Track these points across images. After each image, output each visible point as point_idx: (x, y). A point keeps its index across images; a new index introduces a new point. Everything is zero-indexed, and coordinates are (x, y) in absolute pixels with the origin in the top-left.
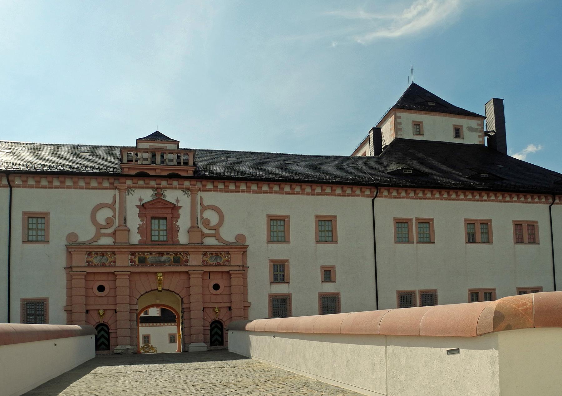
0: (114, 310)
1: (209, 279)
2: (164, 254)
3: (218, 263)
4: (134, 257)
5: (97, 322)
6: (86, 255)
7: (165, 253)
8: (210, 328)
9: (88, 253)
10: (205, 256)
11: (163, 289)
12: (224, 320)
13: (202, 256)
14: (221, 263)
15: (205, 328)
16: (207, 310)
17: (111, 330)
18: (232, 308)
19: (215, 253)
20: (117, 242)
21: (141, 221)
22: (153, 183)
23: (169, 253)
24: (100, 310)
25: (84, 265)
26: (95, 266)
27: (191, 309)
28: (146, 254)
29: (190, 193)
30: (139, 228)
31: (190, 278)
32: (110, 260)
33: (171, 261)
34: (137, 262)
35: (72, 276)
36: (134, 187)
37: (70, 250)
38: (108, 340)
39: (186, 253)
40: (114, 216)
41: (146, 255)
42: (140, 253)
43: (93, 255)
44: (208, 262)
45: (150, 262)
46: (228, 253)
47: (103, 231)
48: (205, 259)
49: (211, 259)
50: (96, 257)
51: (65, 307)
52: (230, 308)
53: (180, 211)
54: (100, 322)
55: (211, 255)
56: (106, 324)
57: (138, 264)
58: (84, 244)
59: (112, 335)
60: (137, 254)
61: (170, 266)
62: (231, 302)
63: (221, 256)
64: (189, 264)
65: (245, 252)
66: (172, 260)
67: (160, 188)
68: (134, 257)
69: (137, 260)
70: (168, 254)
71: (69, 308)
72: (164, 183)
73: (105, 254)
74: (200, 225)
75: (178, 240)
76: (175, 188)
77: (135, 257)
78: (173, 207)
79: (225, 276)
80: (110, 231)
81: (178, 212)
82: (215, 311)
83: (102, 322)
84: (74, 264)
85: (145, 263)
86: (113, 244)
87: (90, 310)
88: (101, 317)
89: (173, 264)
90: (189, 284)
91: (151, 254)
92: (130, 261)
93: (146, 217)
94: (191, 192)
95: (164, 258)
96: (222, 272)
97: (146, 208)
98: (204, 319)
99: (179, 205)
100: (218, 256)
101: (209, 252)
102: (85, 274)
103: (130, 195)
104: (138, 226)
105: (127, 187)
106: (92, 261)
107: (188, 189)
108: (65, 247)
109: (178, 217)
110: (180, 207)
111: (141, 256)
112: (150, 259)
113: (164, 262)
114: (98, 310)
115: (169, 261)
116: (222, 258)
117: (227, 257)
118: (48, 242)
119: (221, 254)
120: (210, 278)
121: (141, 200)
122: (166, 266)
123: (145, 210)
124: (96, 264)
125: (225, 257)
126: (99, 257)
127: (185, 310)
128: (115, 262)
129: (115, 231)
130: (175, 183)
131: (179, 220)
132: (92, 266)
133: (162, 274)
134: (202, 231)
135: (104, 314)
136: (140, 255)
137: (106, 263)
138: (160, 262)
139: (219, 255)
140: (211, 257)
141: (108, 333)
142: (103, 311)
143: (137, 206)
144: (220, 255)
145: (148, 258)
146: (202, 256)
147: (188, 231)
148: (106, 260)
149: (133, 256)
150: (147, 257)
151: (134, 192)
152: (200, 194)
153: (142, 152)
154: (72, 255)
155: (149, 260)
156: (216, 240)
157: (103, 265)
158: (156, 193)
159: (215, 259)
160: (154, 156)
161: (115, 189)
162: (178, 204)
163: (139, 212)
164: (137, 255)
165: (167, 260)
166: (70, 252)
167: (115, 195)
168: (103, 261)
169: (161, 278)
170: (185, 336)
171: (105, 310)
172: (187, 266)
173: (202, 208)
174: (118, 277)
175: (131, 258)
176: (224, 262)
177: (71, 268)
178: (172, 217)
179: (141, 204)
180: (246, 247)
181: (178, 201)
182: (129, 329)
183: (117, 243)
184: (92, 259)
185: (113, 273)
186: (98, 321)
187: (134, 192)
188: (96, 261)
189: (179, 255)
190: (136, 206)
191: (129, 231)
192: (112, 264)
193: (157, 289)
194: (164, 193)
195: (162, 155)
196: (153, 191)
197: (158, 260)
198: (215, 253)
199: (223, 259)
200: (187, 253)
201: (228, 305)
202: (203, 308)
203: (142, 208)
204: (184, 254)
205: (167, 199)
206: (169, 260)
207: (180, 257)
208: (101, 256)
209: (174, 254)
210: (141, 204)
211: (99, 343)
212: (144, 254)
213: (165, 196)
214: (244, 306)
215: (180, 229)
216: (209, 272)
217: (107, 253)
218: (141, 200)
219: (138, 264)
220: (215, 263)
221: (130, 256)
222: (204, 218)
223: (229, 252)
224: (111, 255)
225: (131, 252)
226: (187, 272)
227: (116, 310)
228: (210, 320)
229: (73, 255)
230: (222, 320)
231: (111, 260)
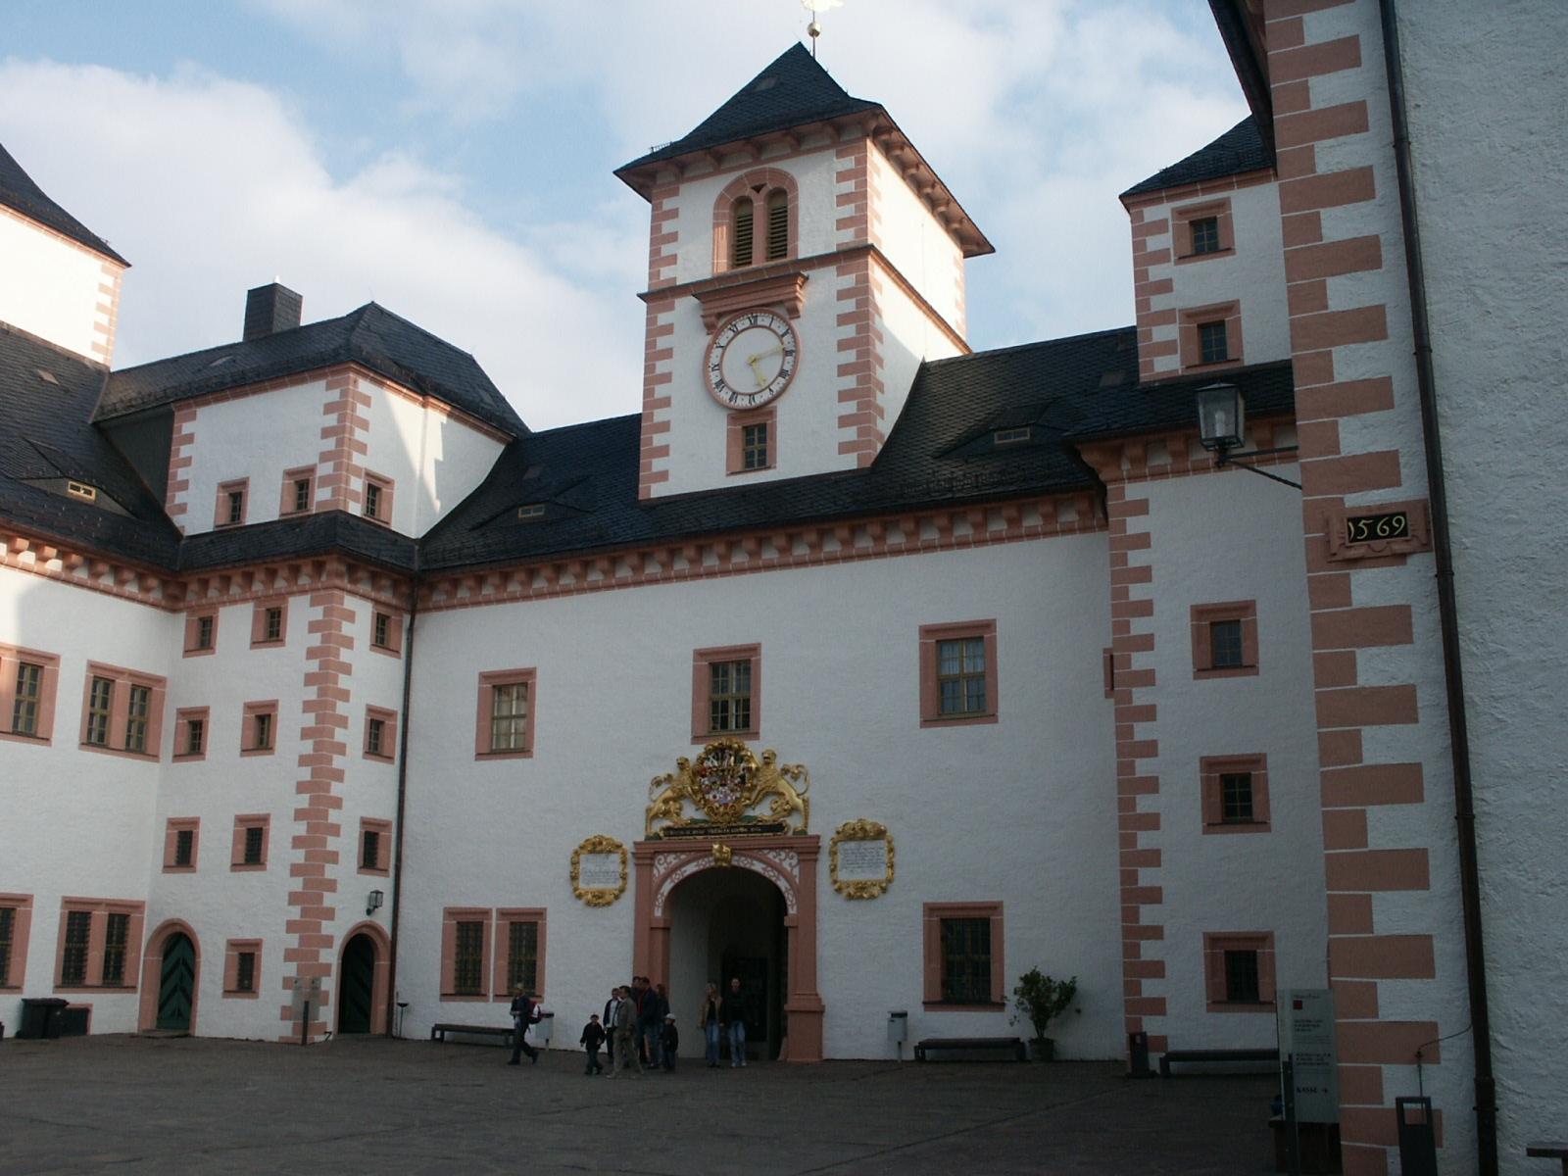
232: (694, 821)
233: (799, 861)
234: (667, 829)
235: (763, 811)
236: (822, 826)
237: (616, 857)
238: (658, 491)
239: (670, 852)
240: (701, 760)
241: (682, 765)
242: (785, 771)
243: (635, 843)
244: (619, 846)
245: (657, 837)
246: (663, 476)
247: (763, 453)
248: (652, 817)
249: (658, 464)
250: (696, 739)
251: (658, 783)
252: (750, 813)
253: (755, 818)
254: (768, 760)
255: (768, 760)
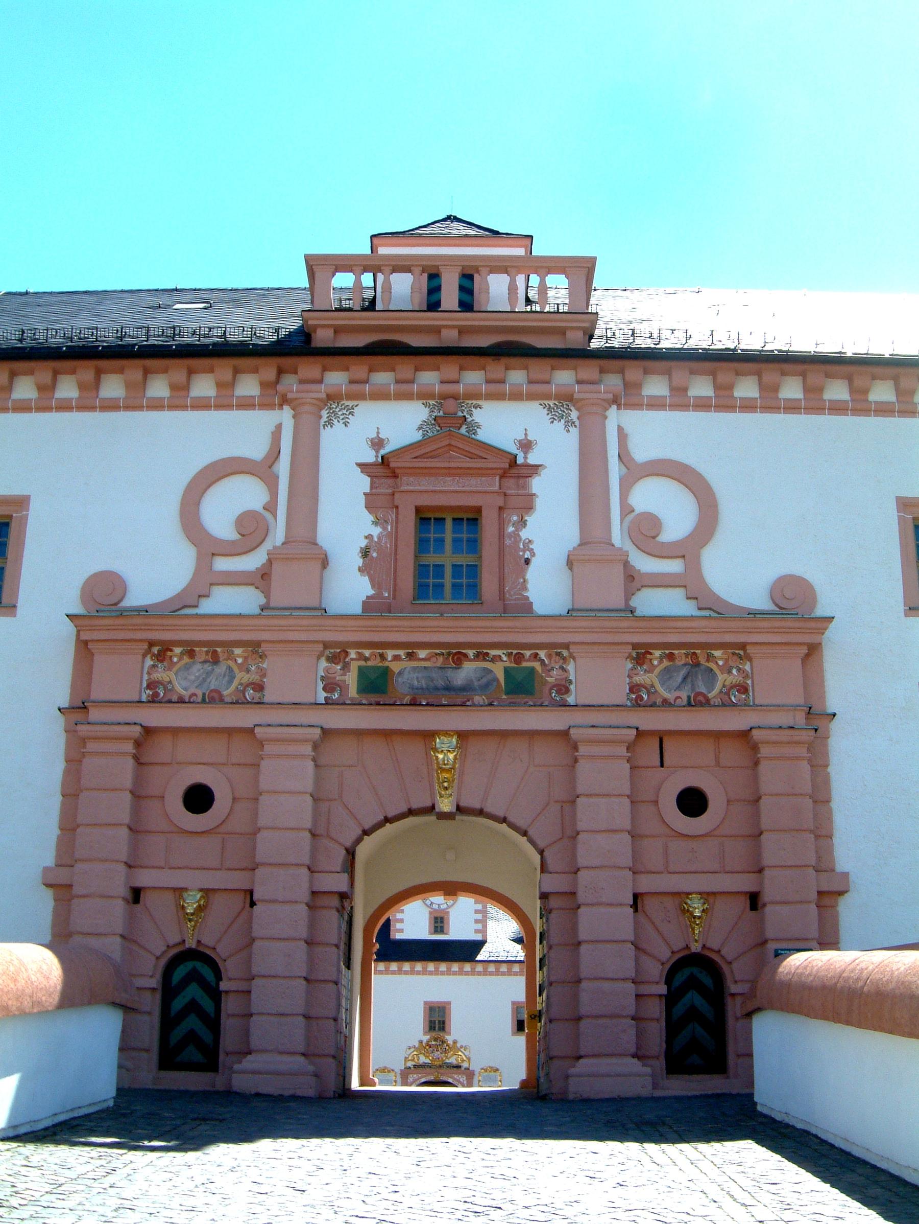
0: (245, 891)
1: (662, 766)
2: (465, 656)
3: (701, 698)
4: (343, 669)
5: (171, 943)
6: (148, 657)
7: (471, 653)
8: (663, 989)
9: (155, 650)
10: (641, 665)
11: (459, 808)
12: (729, 952)
13: (629, 665)
14: (710, 695)
15: (646, 989)
16: (650, 904)
17: (230, 979)
18: (766, 896)
19: (687, 655)
20: (272, 605)
21: (375, 523)
22: (429, 378)
23: (487, 654)
24: (186, 889)
25: (136, 698)
26: (181, 701)
27: (582, 897)
28: (390, 654)
29: (574, 415)
30: (365, 553)
31: (576, 760)
32: (242, 677)
33: (495, 684)
34: (353, 692)
35: (83, 741)
36: (350, 397)
37: (85, 636)
38: (214, 1023)
39: (558, 654)
40: (271, 507)
41: (389, 659)
42: (367, 653)
43: (175, 660)
44: (656, 691)
45: (405, 690)
46: (740, 651)
47: (223, 564)
48: (642, 678)
49: (670, 678)
50: (187, 667)
51: (46, 870)
52: (754, 900)
53: (537, 484)
54: (184, 941)
55: (666, 663)
56: (208, 952)
57: (356, 696)
58: (143, 611)
59: (230, 1005)
60: (353, 654)
61: (491, 705)
62: (760, 871)
63: (711, 665)
64: (571, 700)
65: (813, 651)
66: (497, 680)
67: (455, 397)
68: (339, 667)
69: (351, 679)
70: (481, 656)
71: (63, 876)
72: (473, 378)
73: (222, 657)
74: (617, 536)
75: (527, 598)
76: (516, 396)
77: (346, 667)
78: (507, 466)
79: (732, 754)
80: (252, 562)
81: (525, 486)
82: (686, 912)
83: (194, 946)
84: (94, 696)
85: (384, 693)
86: (258, 611)
87: (144, 888)
88: (190, 920)
89: (504, 697)
90: (574, 788)
91: (411, 656)
92: (321, 685)
93: (397, 507)
94: (578, 409)
95: (469, 670)
96: (717, 736)
97: (397, 471)
98: (637, 947)
99: (532, 459)
100: (697, 665)
101: (657, 646)
102: (137, 735)
103: (338, 426)
104: (364, 543)
105: (324, 396)
106: (170, 682)
107: (567, 398)
108: (69, 629)
109: (527, 505)
110: (535, 469)
111: (370, 663)
112: (406, 676)
113: (466, 688)
114: (179, 891)
115: (487, 685)
116: (715, 675)
117: (739, 670)
118: (15, 606)
119: (709, 657)
120: (666, 763)
121: (377, 443)
122: (474, 705)
123: (390, 481)
124: (186, 694)
125: (730, 672)
126: (199, 666)
127: (553, 902)
128: (259, 687)
129: (270, 562)
130: (517, 377)
131: (530, 519)
132: (170, 702)
133: (454, 740)
134: (626, 564)
135: (200, 909)
136: (366, 659)
137: (225, 693)
138: (448, 688)
139: (702, 660)
140: (667, 670)
141: (216, 995)
142: (199, 896)
143: (363, 467)
144: (708, 660)
145: (400, 673)
146: (629, 665)
147: (570, 563)
148: (227, 678)
149: (337, 664)
150: (396, 667)
151: (352, 414)
152: (614, 418)
153: (387, 270)
154: (93, 654)
155: (400, 679)
156: (688, 598)
157: (213, 699)
158: (441, 413)
159: (685, 679)
160: (434, 290)
161: (281, 407)
162: (525, 458)
163: (368, 490)
164: (352, 659)
165: (476, 684)
166: (86, 643)
167: (279, 427)
168: (213, 684)
169: (451, 756)
170: (551, 1021)
171: (207, 892)
172: (565, 705)
173: (624, 470)
174: (268, 748)
175: (327, 670)
176: (727, 691)
177: (84, 708)
178: (500, 508)
179: (377, 457)
180: (819, 625)
181: (526, 445)
182: (304, 983)
183: (273, 609)
184: (172, 674)
185: (250, 731)
186: (177, 939)
187: (352, 414)
188: (184, 683)
189: (528, 660)
190: (359, 465)
191: (325, 562)
192: (250, 694)
193: (433, 807)
194: (471, 415)
195: (466, 283)
196: (427, 410)
197: (440, 683)
198: (687, 655)
199: (721, 677)
200: (560, 651)
201: (746, 883)
202: (636, 896)
203: (381, 471)
204: (549, 656)
205: (483, 435)
206: (484, 680)
207: (532, 670)
208: (205, 662)
209: (509, 655)
210: (380, 460)
211: (177, 1034)
212: (382, 657)
213: (473, 427)
214: (819, 893)
215: (533, 555)
216: (661, 738)
217: (233, 652)
218: (377, 443)
219: (356, 696)
220: (684, 695)
221: (323, 664)
222: (633, 511)
223: (743, 646)
224: (246, 658)
225: (326, 645)
226: (564, 734)
227: (251, 892)
228: (664, 953)
229: (97, 658)
230: (719, 951)
231: (246, 678)
232: (426, 1063)
233: (467, 1079)
234: (414, 1066)
235: (453, 1060)
236: (475, 1066)
237: (392, 1074)
238: (399, 936)
239: (415, 1074)
240: (428, 1042)
241: (421, 1042)
242: (462, 1047)
243: (401, 1070)
244: (393, 1070)
245: (410, 1068)
246: (401, 931)
247: (442, 927)
248: (406, 1059)
249: (399, 926)
250: (425, 1033)
251: (410, 1048)
252: (447, 1061)
253: (449, 1063)
254: (455, 1042)
255: (455, 1042)
